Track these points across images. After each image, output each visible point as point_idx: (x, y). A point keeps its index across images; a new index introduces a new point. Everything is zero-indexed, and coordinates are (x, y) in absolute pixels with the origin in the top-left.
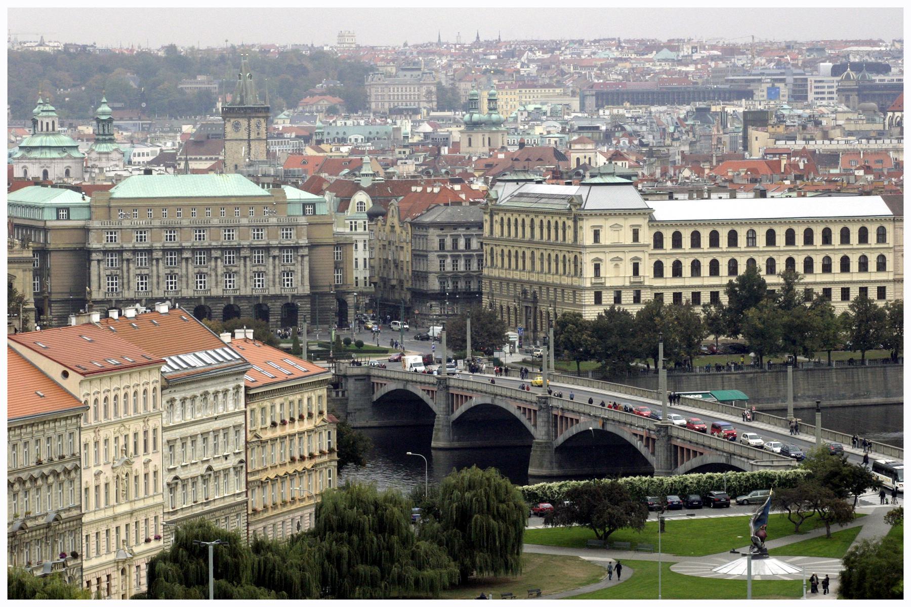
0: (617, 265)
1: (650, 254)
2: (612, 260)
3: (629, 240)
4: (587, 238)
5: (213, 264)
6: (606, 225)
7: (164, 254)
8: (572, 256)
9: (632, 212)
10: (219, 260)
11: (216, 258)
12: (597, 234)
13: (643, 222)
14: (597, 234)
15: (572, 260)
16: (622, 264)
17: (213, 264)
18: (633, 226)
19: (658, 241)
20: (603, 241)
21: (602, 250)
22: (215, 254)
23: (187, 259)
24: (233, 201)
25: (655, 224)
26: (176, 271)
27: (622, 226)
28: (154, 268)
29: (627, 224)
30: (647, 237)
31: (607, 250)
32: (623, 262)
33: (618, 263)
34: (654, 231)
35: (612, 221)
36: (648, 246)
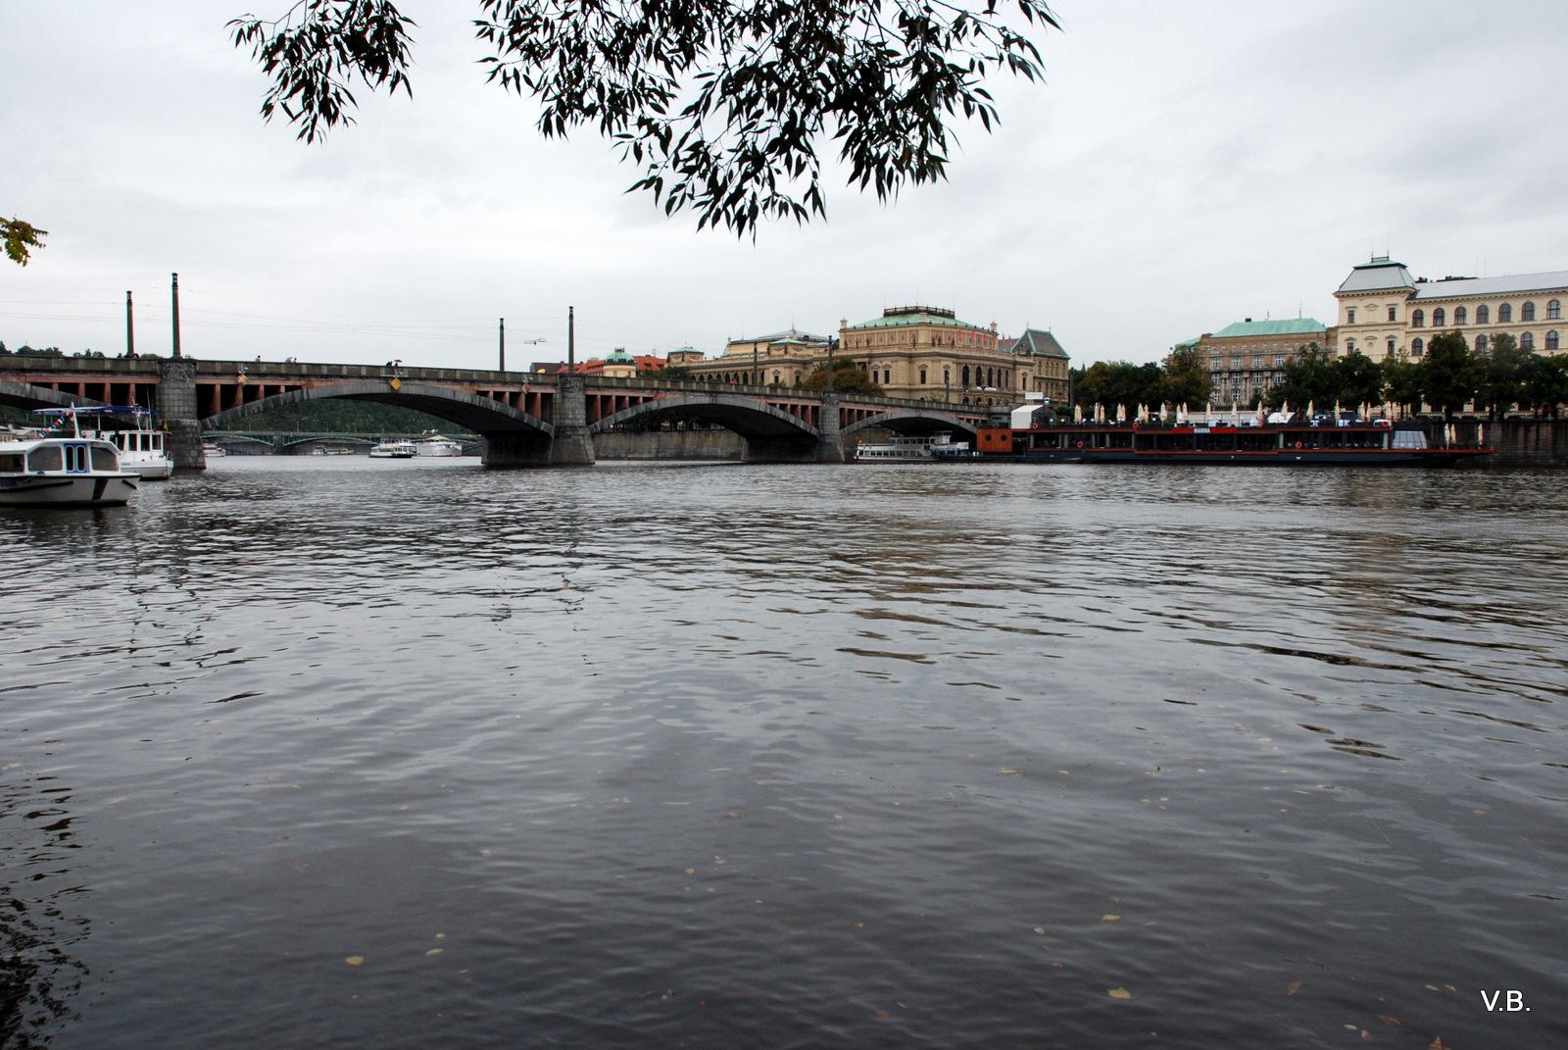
0: (1371, 343)
1: (1407, 333)
2: (1367, 339)
3: (1385, 319)
5: (1265, 382)
7: (1230, 376)
9: (1386, 291)
10: (1269, 380)
11: (1267, 378)
13: (1399, 301)
16: (1376, 343)
17: (1265, 382)
18: (1388, 305)
19: (1418, 318)
20: (1357, 321)
21: (1357, 329)
22: (1268, 374)
23: (1246, 379)
24: (1294, 336)
26: (1239, 387)
28: (1223, 385)
29: (1382, 305)
30: (1404, 314)
31: (1360, 329)
34: (1413, 309)
36: (1405, 324)
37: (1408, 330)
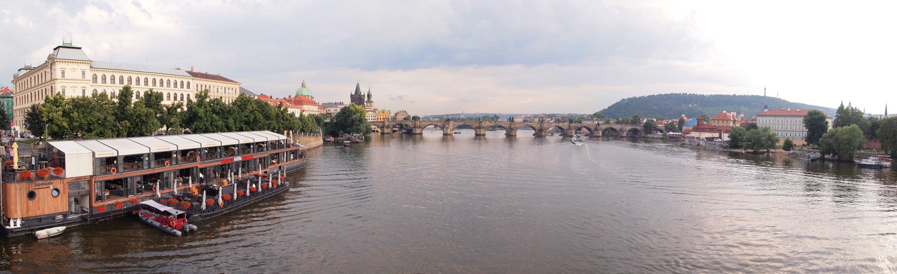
1: (91, 85)
3: (80, 77)
4: (58, 75)
6: (68, 67)
8: (50, 87)
12: (63, 73)
13: (86, 67)
14: (63, 73)
15: (50, 89)
19: (95, 78)
25: (93, 69)
27: (76, 69)
30: (89, 75)
32: (77, 88)
33: (74, 89)
34: (93, 73)
35: (72, 66)
37: (91, 84)
